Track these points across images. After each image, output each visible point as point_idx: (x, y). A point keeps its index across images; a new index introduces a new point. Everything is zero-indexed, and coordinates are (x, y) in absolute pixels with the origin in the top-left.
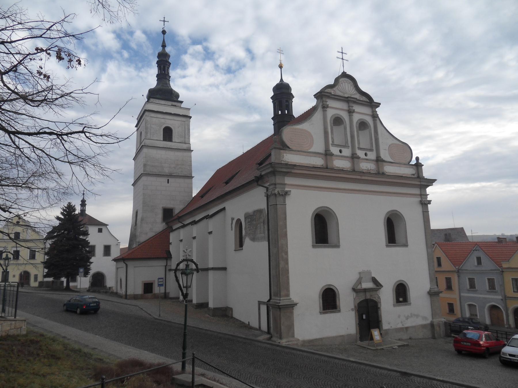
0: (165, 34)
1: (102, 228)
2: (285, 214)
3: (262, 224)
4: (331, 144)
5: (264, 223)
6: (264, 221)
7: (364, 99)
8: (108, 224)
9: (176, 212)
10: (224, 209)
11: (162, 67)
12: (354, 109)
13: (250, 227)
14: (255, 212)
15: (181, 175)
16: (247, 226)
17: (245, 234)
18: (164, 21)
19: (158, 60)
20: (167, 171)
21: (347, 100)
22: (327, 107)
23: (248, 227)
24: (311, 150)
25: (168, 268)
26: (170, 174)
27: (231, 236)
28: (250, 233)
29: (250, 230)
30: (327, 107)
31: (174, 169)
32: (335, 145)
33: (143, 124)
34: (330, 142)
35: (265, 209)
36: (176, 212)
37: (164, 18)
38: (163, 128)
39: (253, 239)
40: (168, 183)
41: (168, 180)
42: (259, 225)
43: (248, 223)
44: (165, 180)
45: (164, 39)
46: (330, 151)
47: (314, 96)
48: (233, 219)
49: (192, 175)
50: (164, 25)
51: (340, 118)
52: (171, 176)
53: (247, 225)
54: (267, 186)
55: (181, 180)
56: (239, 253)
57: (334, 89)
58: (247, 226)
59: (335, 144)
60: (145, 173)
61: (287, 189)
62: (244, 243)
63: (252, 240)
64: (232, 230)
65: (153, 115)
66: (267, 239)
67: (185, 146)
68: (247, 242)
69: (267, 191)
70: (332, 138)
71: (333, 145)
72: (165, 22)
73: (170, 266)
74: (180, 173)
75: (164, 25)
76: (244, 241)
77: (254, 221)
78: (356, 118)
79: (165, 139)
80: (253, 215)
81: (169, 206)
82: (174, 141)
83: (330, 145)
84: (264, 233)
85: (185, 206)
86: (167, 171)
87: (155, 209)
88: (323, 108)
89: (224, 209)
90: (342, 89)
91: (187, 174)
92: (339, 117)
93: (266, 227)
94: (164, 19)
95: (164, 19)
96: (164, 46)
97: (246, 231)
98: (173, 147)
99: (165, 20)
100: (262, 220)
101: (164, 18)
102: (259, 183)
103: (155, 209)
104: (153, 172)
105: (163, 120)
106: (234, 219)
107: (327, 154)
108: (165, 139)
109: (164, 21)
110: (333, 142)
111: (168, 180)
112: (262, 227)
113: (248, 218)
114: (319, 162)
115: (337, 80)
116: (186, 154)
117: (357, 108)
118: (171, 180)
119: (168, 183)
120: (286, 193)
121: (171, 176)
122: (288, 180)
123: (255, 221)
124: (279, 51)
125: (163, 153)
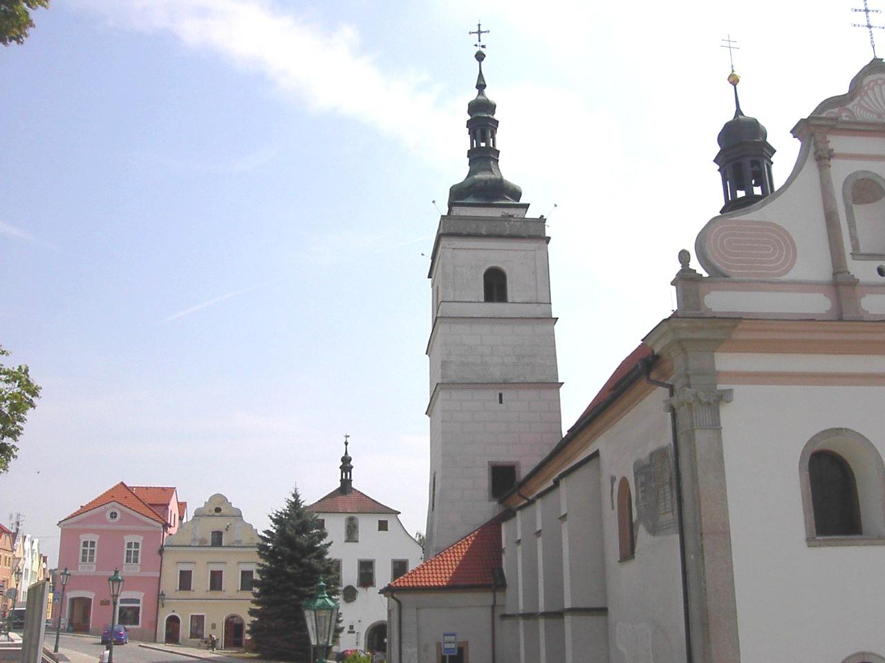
0: (482, 60)
1: (386, 519)
3: (668, 486)
4: (851, 254)
8: (399, 511)
9: (523, 472)
10: (596, 454)
11: (479, 132)
15: (529, 380)
16: (640, 496)
18: (479, 32)
19: (469, 118)
20: (497, 374)
22: (831, 155)
24: (792, 275)
25: (499, 612)
30: (831, 155)
32: (862, 255)
33: (438, 271)
34: (848, 248)
36: (523, 472)
38: (483, 273)
39: (653, 531)
40: (501, 402)
41: (501, 395)
43: (641, 487)
44: (492, 395)
45: (480, 72)
46: (849, 273)
47: (791, 132)
49: (557, 379)
50: (479, 41)
51: (874, 182)
52: (506, 384)
53: (640, 490)
54: (671, 383)
55: (532, 394)
57: (850, 106)
58: (640, 496)
59: (862, 252)
60: (445, 381)
61: (720, 387)
63: (650, 533)
66: (677, 528)
67: (537, 311)
68: (642, 536)
69: (672, 394)
70: (854, 238)
71: (856, 255)
73: (503, 606)
75: (479, 41)
79: (489, 297)
81: (504, 458)
82: (510, 299)
83: (848, 258)
88: (817, 160)
89: (596, 454)
90: (874, 104)
92: (869, 180)
94: (479, 28)
95: (479, 28)
101: (479, 25)
102: (654, 376)
108: (489, 297)
110: (855, 246)
111: (501, 395)
114: (819, 304)
115: (856, 84)
119: (501, 402)
122: (726, 362)
124: (727, 44)
125: (484, 329)
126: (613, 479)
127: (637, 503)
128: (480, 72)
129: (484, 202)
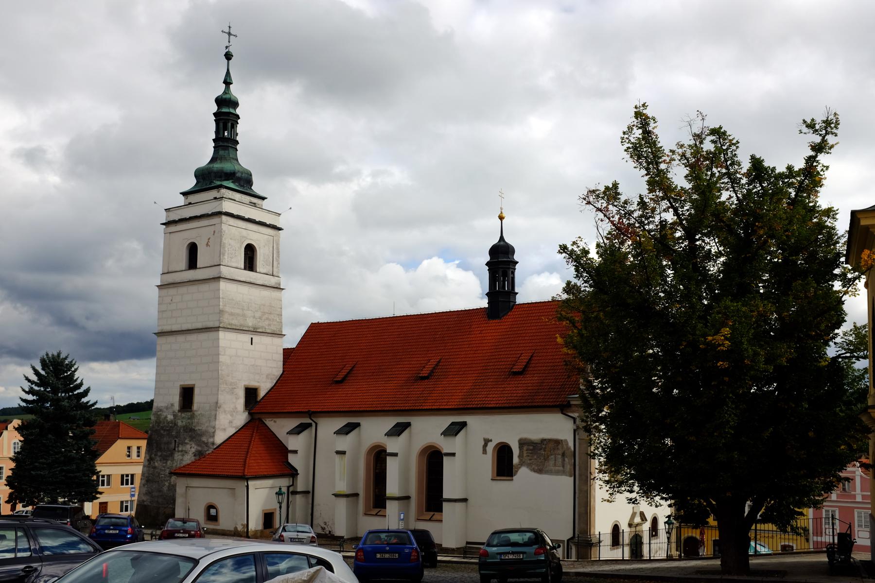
0: (231, 59)
14: (543, 440)
18: (229, 34)
20: (250, 323)
26: (254, 328)
31: (259, 320)
37: (230, 27)
40: (252, 344)
44: (246, 338)
45: (228, 70)
48: (487, 442)
65: (232, 221)
67: (272, 281)
72: (231, 37)
74: (267, 327)
75: (229, 42)
81: (253, 384)
82: (258, 270)
85: (274, 384)
86: (250, 324)
87: (235, 388)
91: (275, 329)
94: (230, 30)
95: (230, 30)
96: (227, 82)
98: (258, 282)
99: (232, 32)
103: (235, 388)
104: (232, 324)
105: (244, 233)
109: (229, 34)
116: (275, 294)
118: (256, 339)
119: (252, 344)
121: (255, 331)
125: (244, 289)
128: (228, 70)
129: (237, 188)
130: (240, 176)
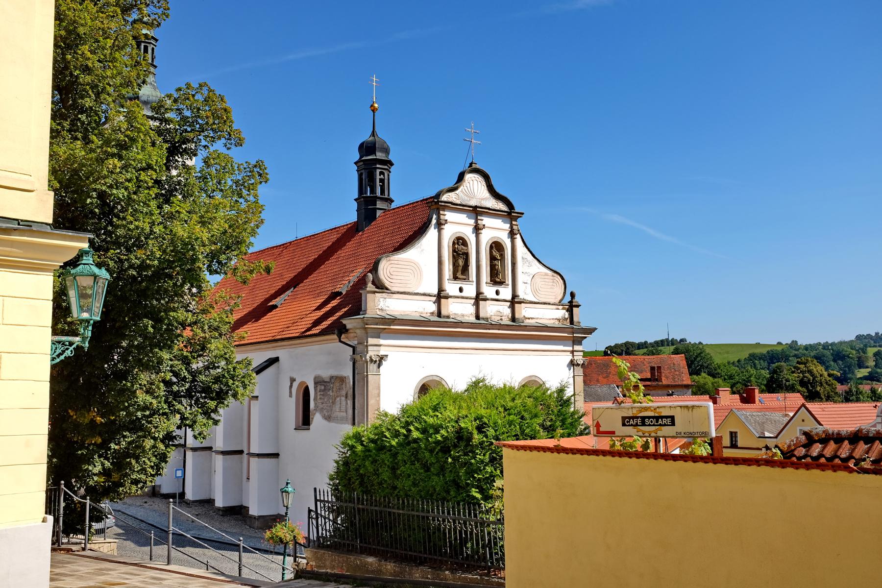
2: (379, 388)
5: (346, 397)
6: (347, 394)
7: (501, 206)
12: (484, 224)
13: (324, 399)
16: (319, 397)
17: (315, 407)
21: (476, 211)
23: (320, 398)
27: (290, 409)
28: (323, 408)
29: (323, 403)
35: (348, 376)
39: (328, 418)
42: (338, 399)
53: (319, 394)
56: (303, 434)
61: (382, 353)
62: (312, 421)
64: (291, 396)
68: (317, 419)
76: (313, 418)
77: (331, 391)
78: (487, 237)
80: (329, 382)
83: (447, 281)
84: (346, 412)
93: (350, 403)
97: (316, 404)
100: (344, 393)
106: (295, 380)
107: (440, 296)
112: (344, 403)
113: (321, 385)
114: (428, 307)
117: (486, 221)
120: (382, 358)
123: (333, 391)
126: (293, 380)
127: (315, 399)
130: (146, 100)
